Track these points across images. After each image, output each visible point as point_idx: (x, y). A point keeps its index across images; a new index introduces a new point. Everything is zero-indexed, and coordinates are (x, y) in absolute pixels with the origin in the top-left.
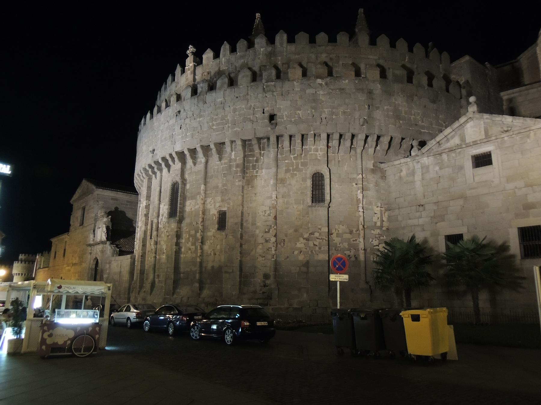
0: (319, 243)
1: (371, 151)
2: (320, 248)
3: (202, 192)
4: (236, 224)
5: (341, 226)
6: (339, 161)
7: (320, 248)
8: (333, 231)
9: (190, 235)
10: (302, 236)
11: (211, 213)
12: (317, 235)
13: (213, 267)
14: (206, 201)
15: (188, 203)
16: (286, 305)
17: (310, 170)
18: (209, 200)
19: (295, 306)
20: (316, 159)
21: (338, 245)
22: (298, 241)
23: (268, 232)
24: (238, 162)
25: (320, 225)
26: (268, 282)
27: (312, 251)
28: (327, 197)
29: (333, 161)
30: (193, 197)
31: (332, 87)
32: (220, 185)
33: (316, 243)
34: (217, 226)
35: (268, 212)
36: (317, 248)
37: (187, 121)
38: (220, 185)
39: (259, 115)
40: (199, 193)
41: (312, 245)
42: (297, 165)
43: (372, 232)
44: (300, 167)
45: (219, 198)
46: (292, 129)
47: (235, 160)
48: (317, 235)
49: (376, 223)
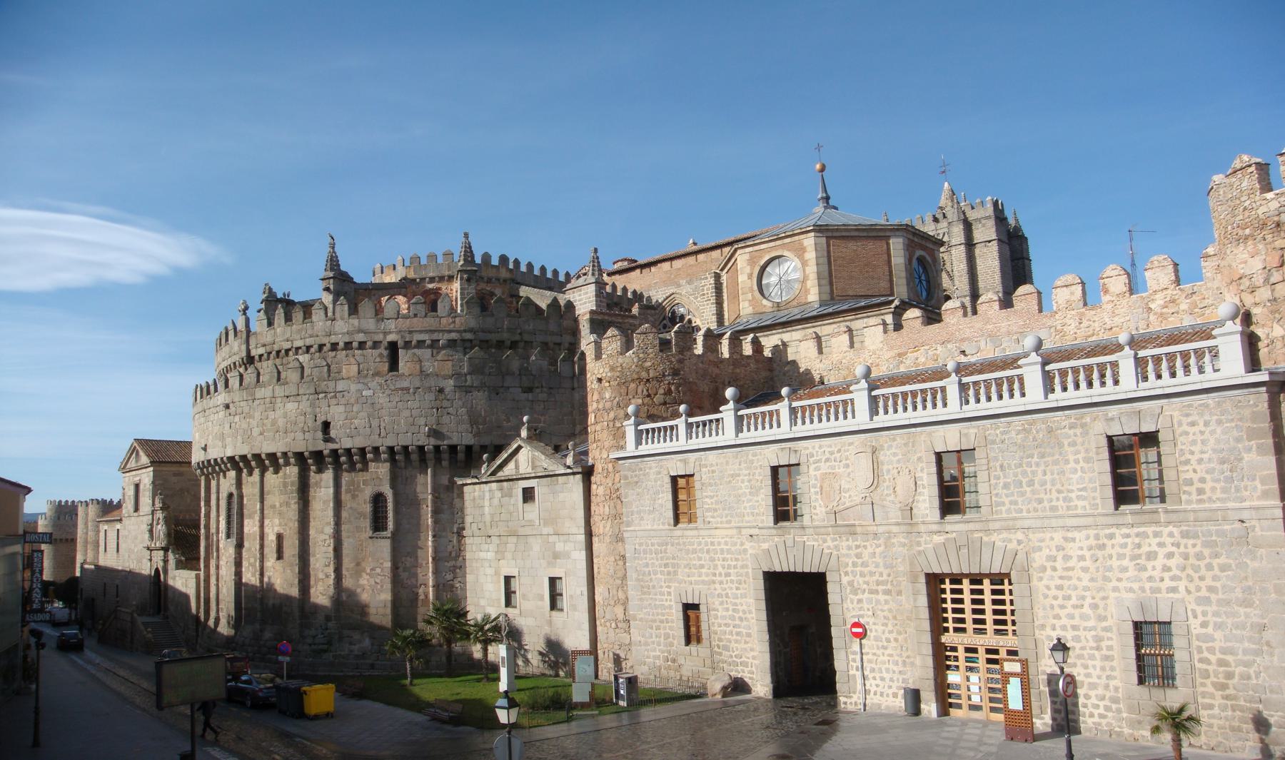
0: (381, 580)
1: (445, 463)
2: (382, 586)
3: (258, 512)
4: (294, 556)
5: (408, 559)
6: (407, 478)
7: (382, 586)
8: (400, 565)
9: (250, 564)
10: (364, 570)
11: (270, 538)
12: (378, 570)
13: (274, 605)
14: (263, 523)
15: (246, 522)
16: (346, 652)
17: (368, 493)
18: (267, 522)
19: (356, 653)
20: (378, 478)
21: (405, 582)
22: (361, 576)
23: (329, 566)
24: (293, 479)
25: (382, 559)
26: (330, 624)
27: (373, 590)
28: (391, 525)
29: (400, 479)
30: (251, 517)
31: (393, 388)
32: (278, 504)
33: (378, 581)
34: (275, 556)
35: (328, 542)
36: (379, 587)
37: (237, 418)
38: (278, 504)
39: (310, 423)
40: (255, 512)
41: (373, 583)
42: (359, 483)
43: (446, 564)
44: (362, 486)
45: (277, 521)
46: (347, 443)
47: (290, 477)
48: (378, 570)
49: (451, 553)
